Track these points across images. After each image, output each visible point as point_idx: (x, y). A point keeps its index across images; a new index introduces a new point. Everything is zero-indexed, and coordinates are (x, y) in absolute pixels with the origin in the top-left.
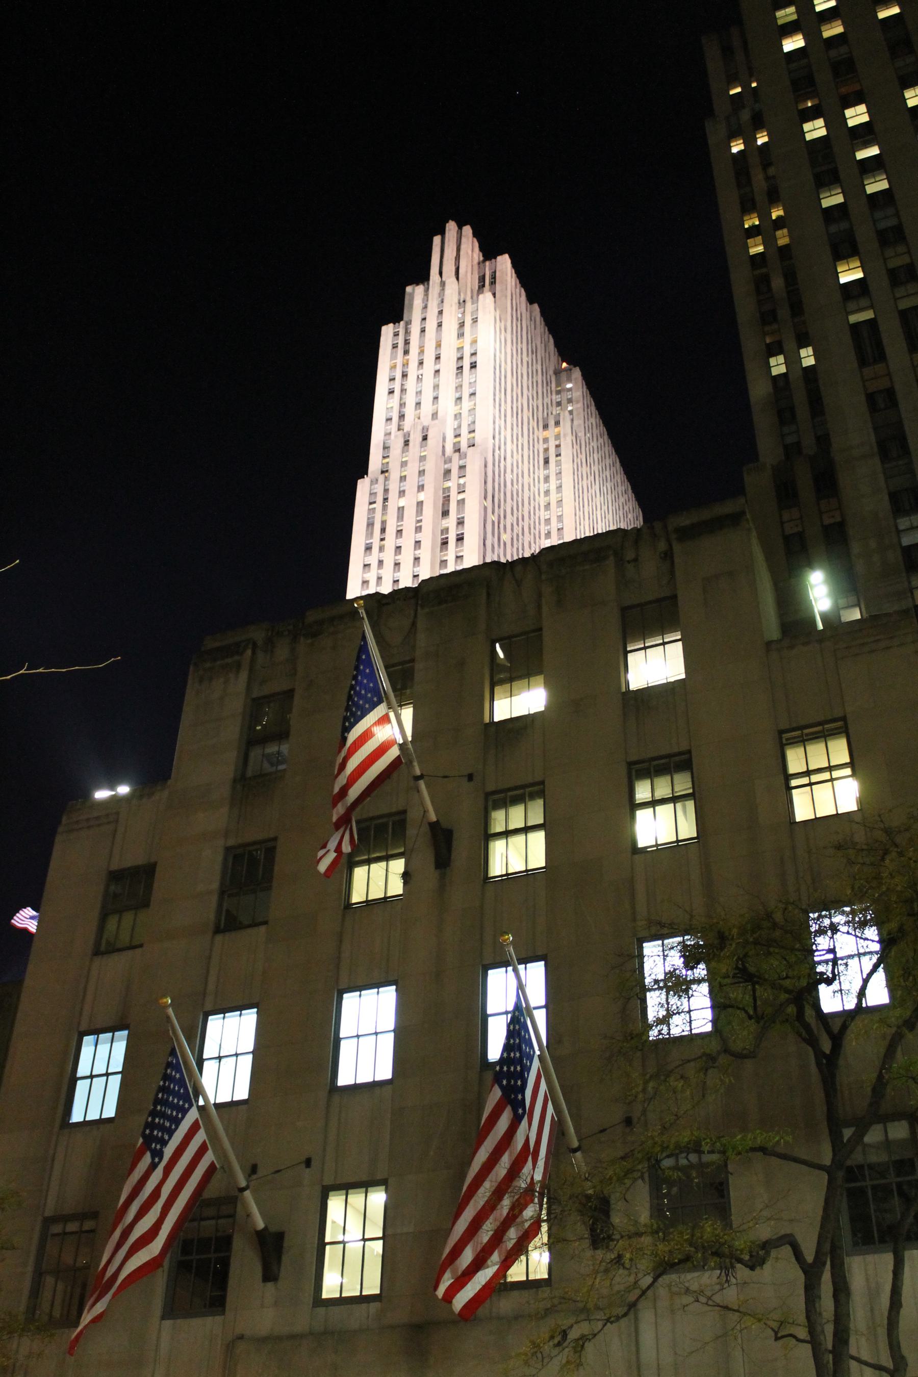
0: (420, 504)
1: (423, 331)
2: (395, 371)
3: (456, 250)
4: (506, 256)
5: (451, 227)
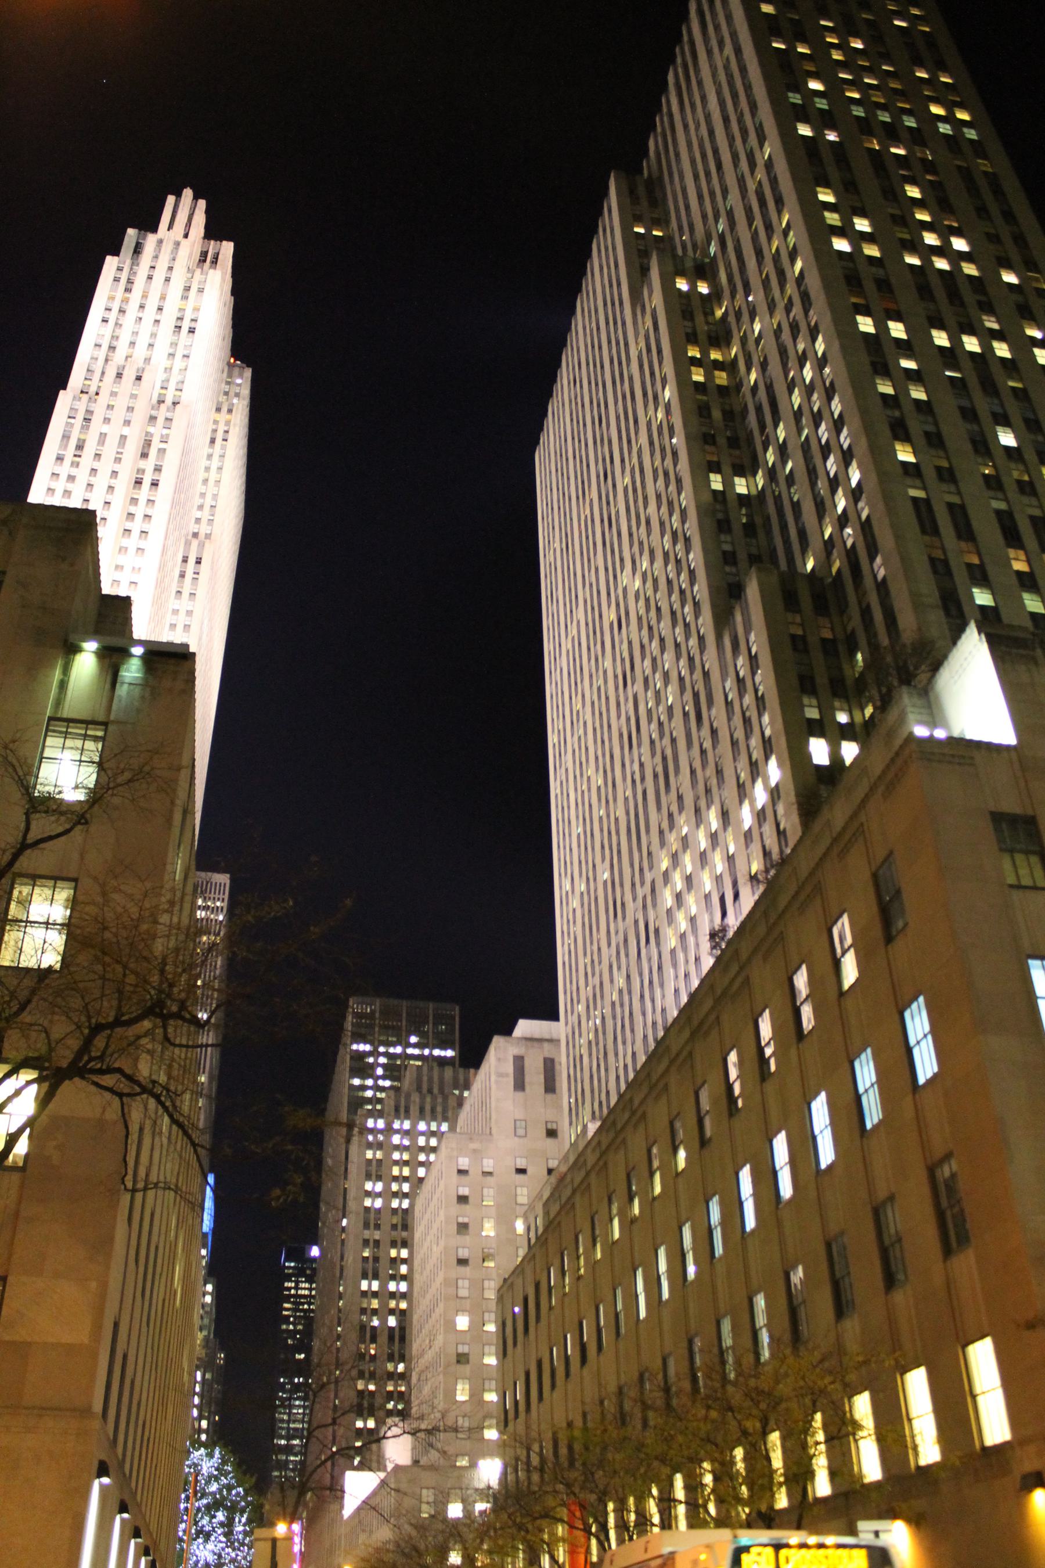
0: (123, 438)
3: (184, 216)
4: (231, 245)
5: (188, 193)
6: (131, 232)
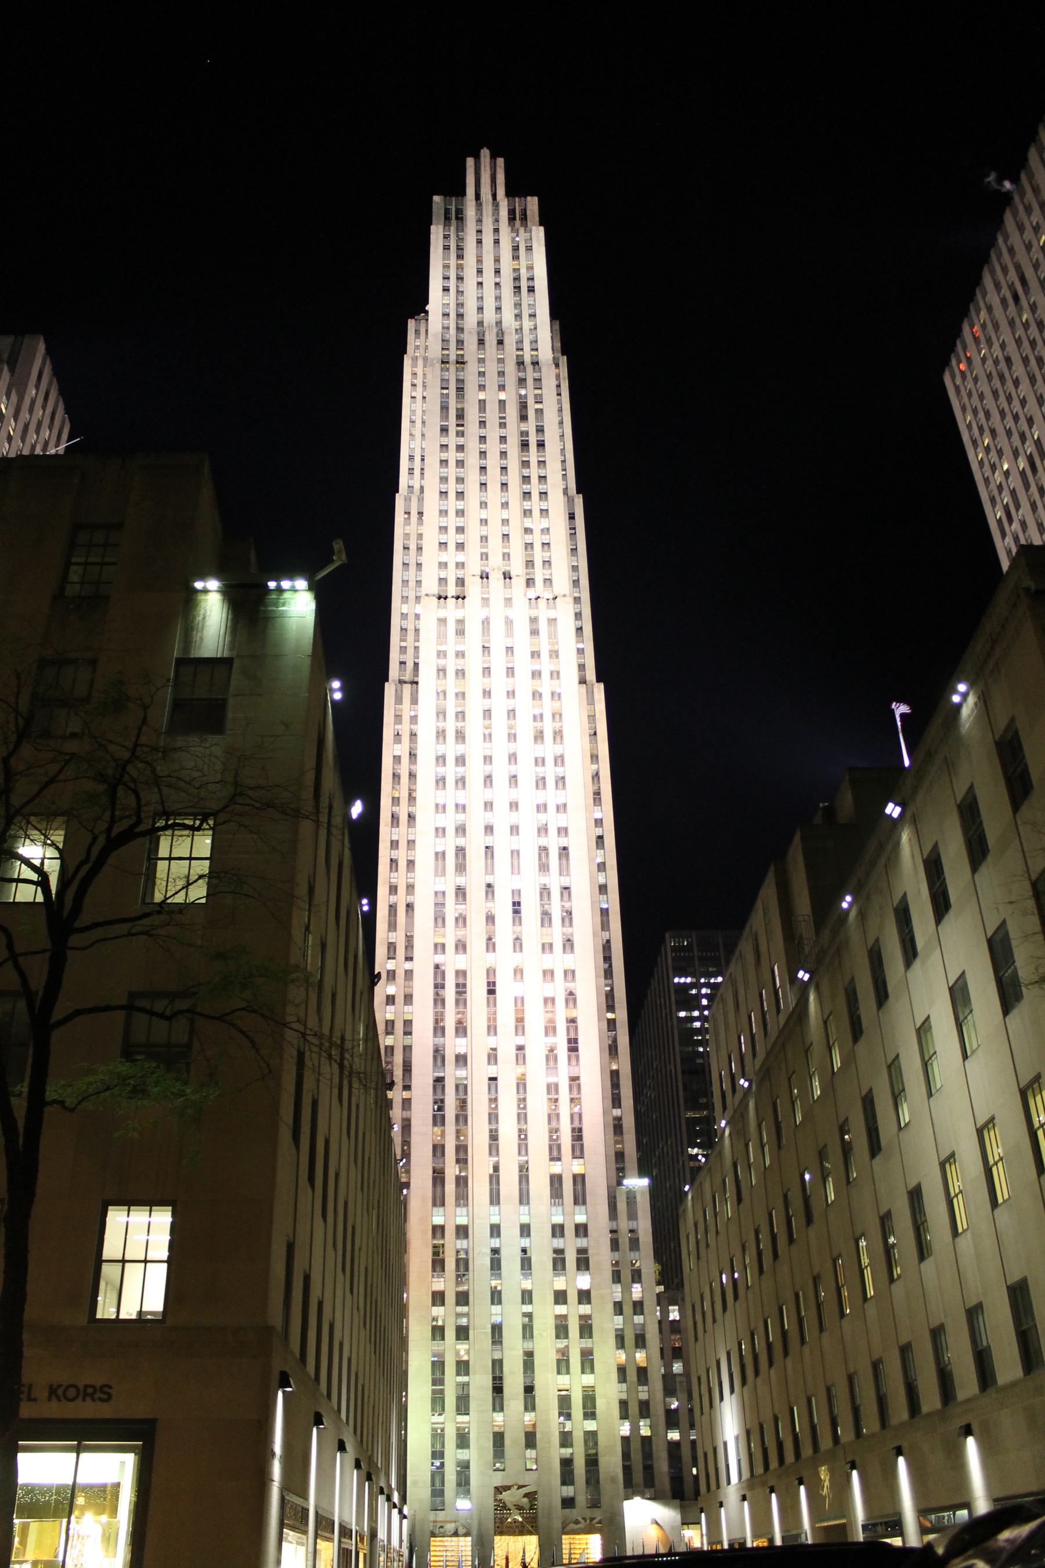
0: (502, 403)
1: (479, 242)
2: (449, 271)
3: (485, 174)
4: (536, 199)
5: (485, 153)
6: (437, 199)
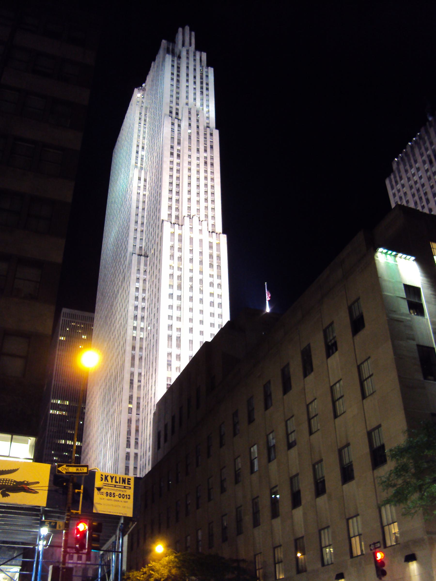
3: (185, 37)
5: (187, 28)
